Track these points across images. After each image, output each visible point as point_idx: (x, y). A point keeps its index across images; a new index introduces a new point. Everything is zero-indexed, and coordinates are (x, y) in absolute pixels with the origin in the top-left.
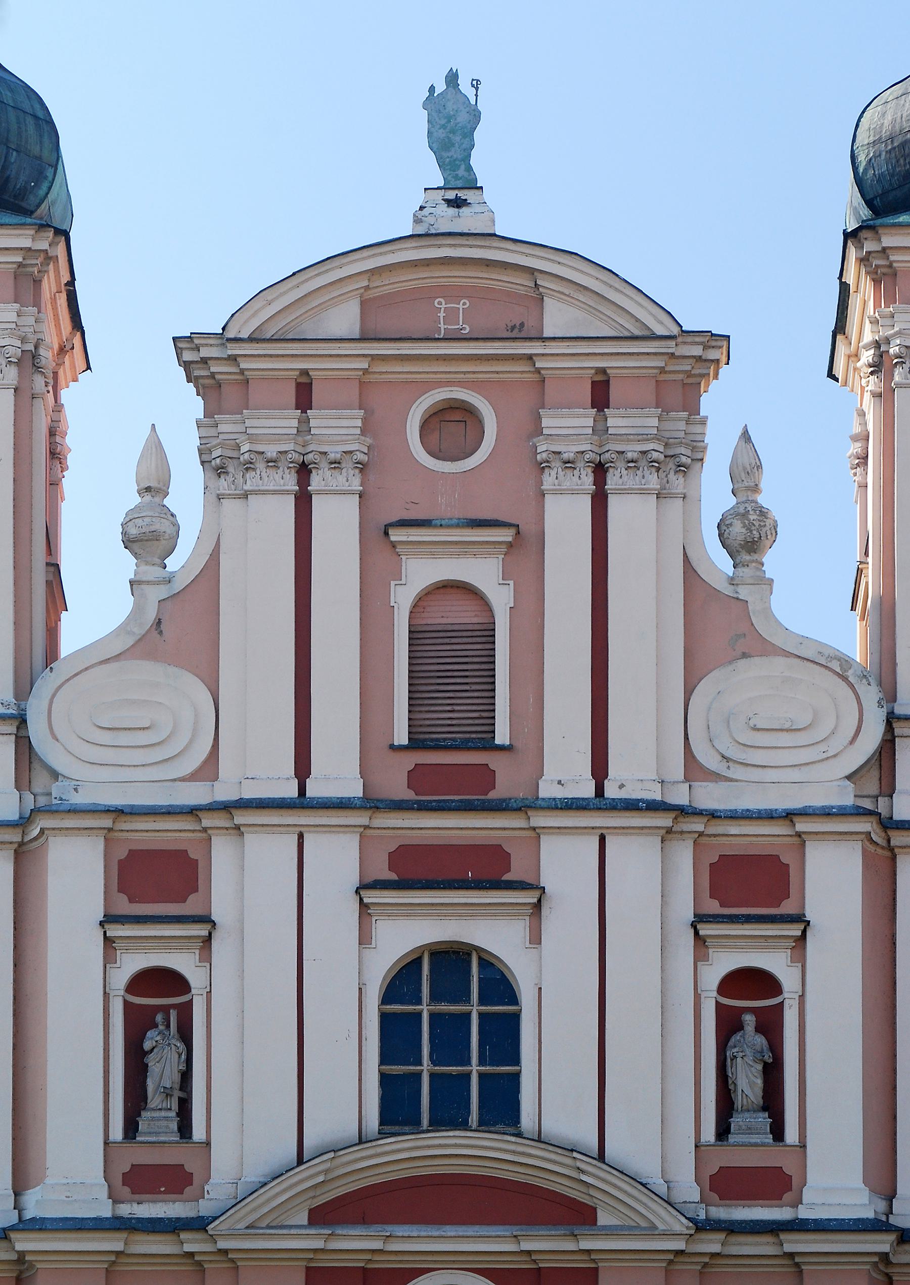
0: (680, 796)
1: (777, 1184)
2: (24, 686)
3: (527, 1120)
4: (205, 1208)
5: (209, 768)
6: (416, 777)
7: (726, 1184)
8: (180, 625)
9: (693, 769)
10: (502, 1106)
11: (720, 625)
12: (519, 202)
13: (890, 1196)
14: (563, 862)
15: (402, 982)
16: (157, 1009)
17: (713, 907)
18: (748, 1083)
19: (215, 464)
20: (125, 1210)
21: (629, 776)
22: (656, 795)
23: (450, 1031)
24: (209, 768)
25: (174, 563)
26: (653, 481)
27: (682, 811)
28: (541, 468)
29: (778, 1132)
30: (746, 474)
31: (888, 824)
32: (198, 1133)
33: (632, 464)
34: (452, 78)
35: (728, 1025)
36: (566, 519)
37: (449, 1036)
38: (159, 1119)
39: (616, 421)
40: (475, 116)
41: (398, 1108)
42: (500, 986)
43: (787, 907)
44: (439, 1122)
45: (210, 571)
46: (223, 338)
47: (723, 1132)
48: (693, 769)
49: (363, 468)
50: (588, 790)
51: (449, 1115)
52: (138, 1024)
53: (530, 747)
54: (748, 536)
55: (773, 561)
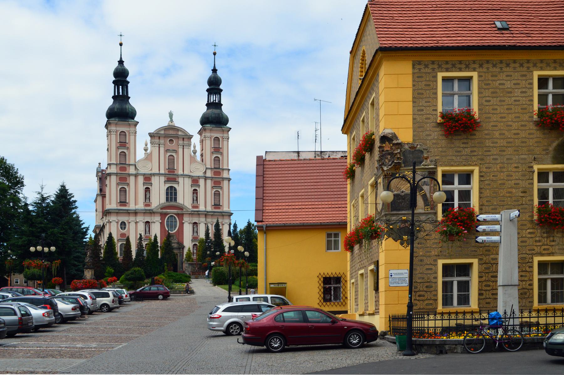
5: (151, 170)
8: (149, 157)
9: (191, 172)
10: (176, 200)
11: (193, 159)
12: (177, 123)
13: (206, 208)
14: (181, 180)
15: (167, 189)
16: (147, 190)
18: (195, 198)
21: (186, 172)
23: (171, 193)
24: (151, 170)
35: (193, 193)
37: (171, 194)
38: (147, 200)
41: (167, 200)
42: (175, 189)
45: (151, 153)
48: (191, 172)
51: (171, 200)
53: (178, 170)
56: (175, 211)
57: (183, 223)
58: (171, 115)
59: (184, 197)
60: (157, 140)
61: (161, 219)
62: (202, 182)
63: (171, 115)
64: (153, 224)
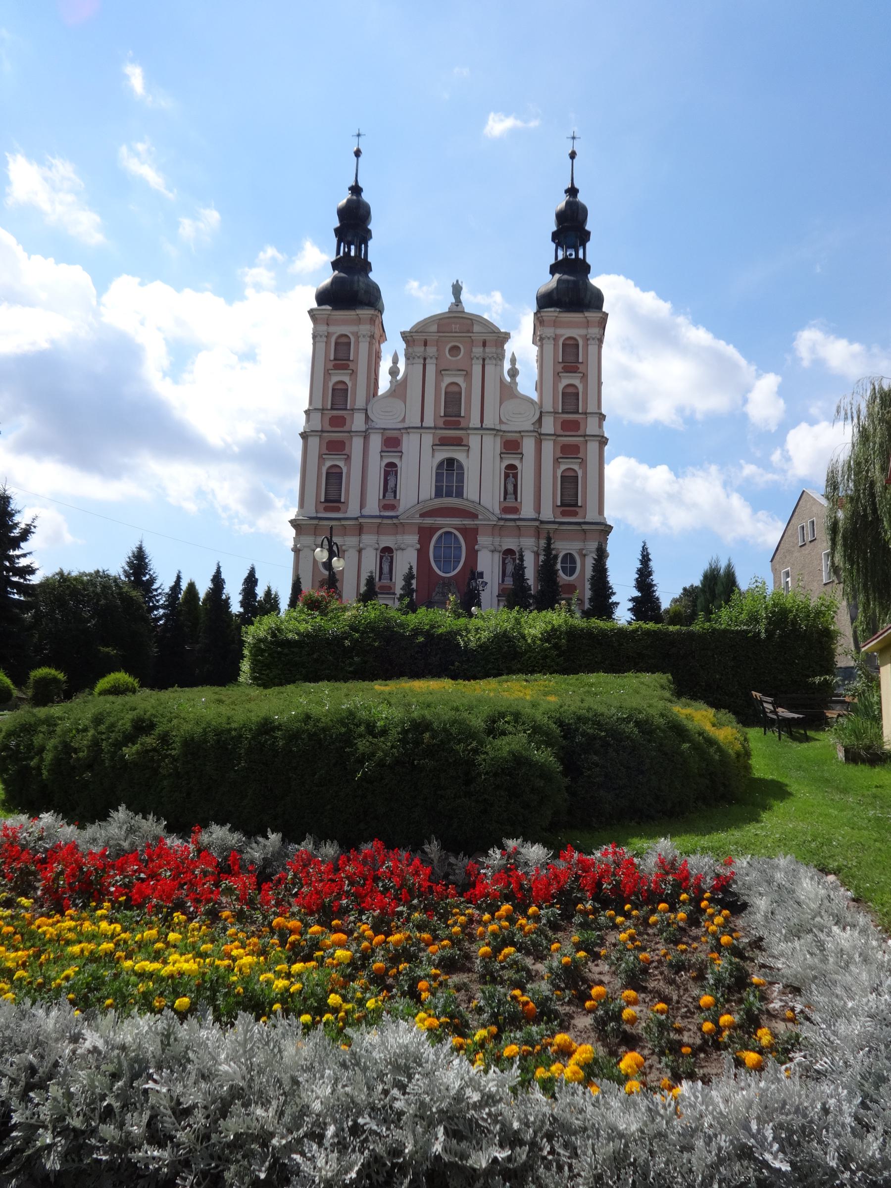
0: (498, 427)
1: (516, 510)
2: (368, 402)
3: (465, 496)
4: (398, 513)
5: (403, 420)
6: (445, 423)
7: (505, 510)
8: (399, 389)
9: (501, 422)
10: (460, 494)
11: (508, 391)
14: (474, 441)
16: (391, 470)
17: (504, 451)
18: (510, 488)
19: (408, 357)
20: (382, 514)
21: (488, 423)
22: (493, 427)
24: (403, 420)
25: (399, 378)
26: (494, 362)
27: (498, 430)
28: (472, 359)
29: (516, 499)
30: (513, 360)
31: (540, 434)
32: (398, 498)
33: (490, 358)
34: (457, 281)
35: (507, 476)
36: (477, 369)
38: (390, 495)
39: (487, 350)
40: (461, 288)
41: (439, 493)
42: (461, 467)
43: (519, 451)
44: (446, 496)
46: (410, 332)
47: (505, 499)
48: (501, 422)
49: (437, 358)
50: (479, 426)
51: (449, 495)
52: (387, 474)
54: (514, 373)
55: (518, 379)
56: (456, 521)
57: (477, 551)
58: (457, 290)
59: (482, 486)
60: (419, 350)
61: (420, 542)
62: (528, 446)
63: (457, 290)
64: (399, 552)
